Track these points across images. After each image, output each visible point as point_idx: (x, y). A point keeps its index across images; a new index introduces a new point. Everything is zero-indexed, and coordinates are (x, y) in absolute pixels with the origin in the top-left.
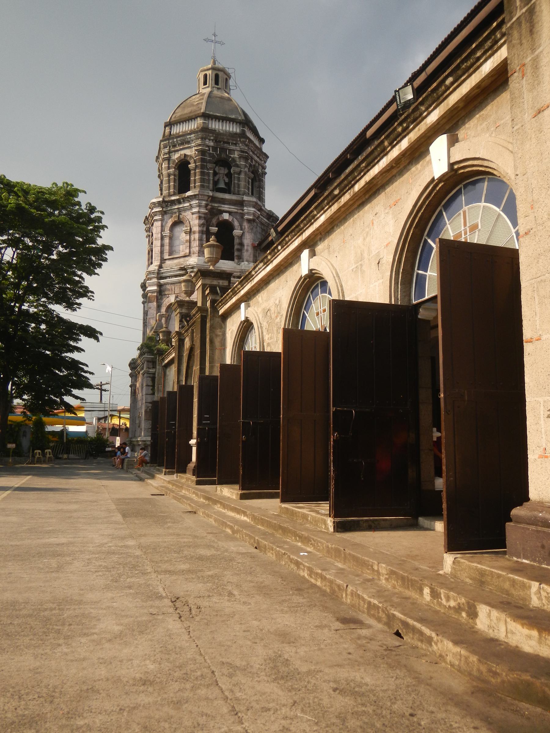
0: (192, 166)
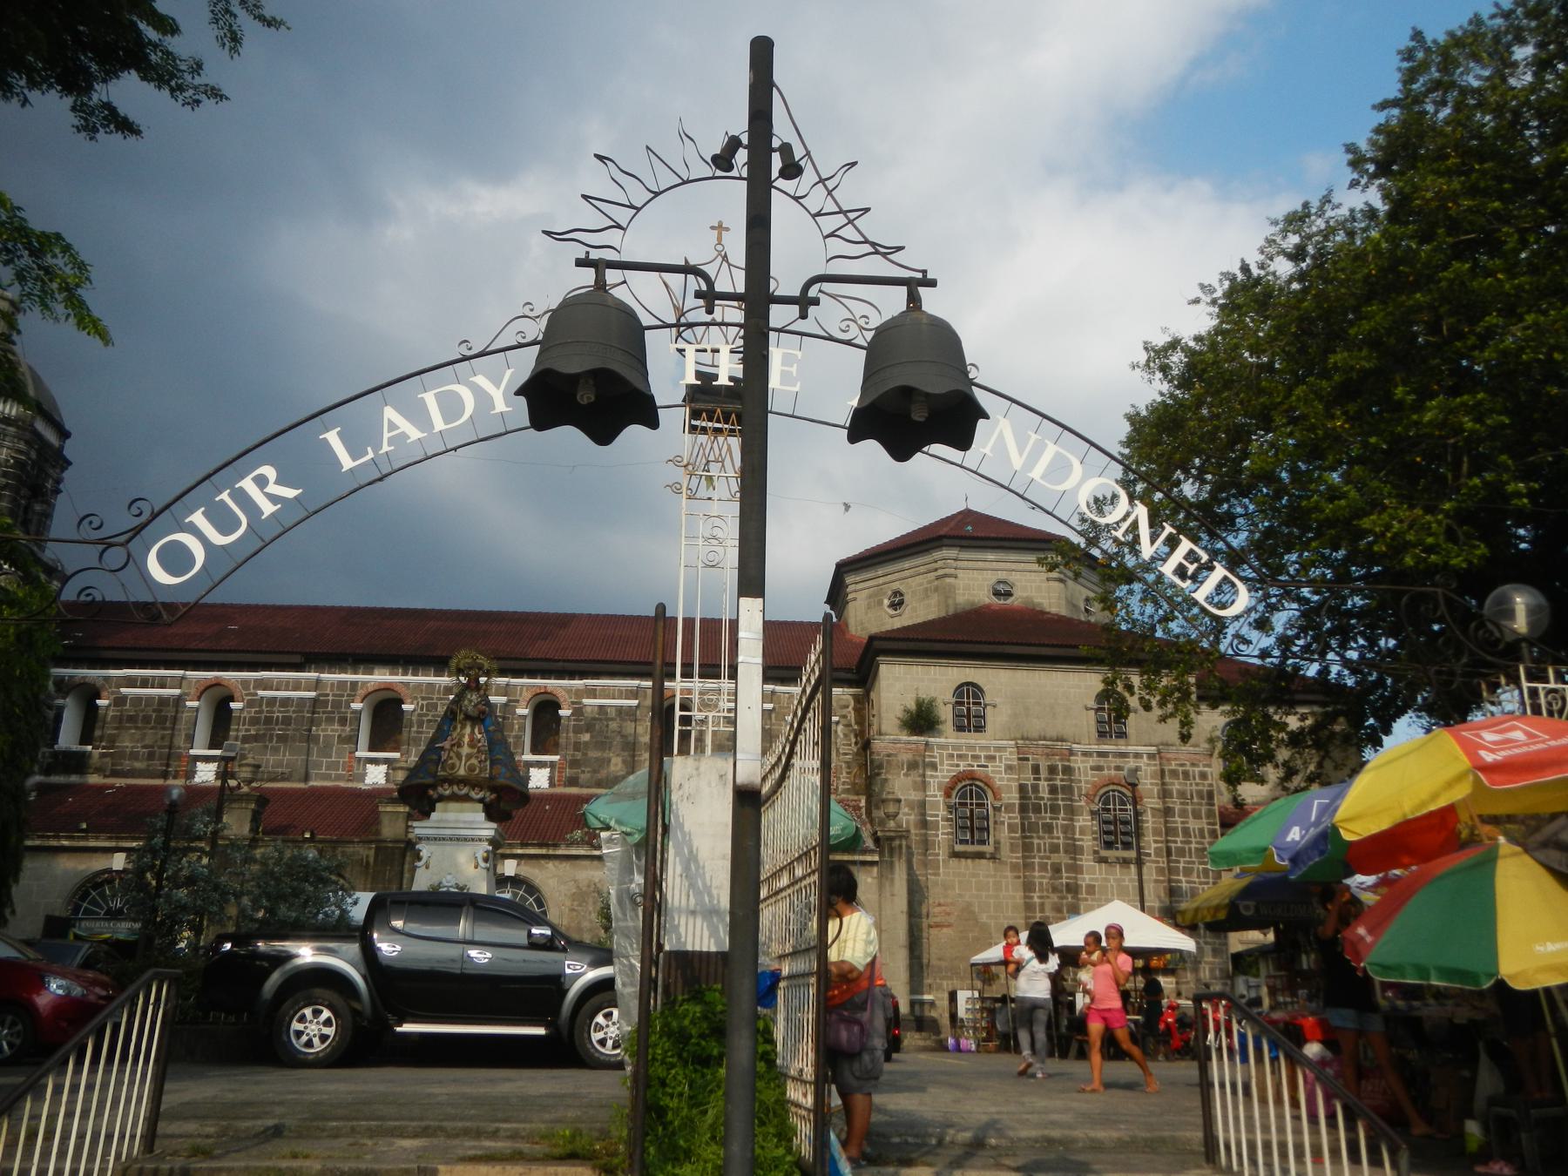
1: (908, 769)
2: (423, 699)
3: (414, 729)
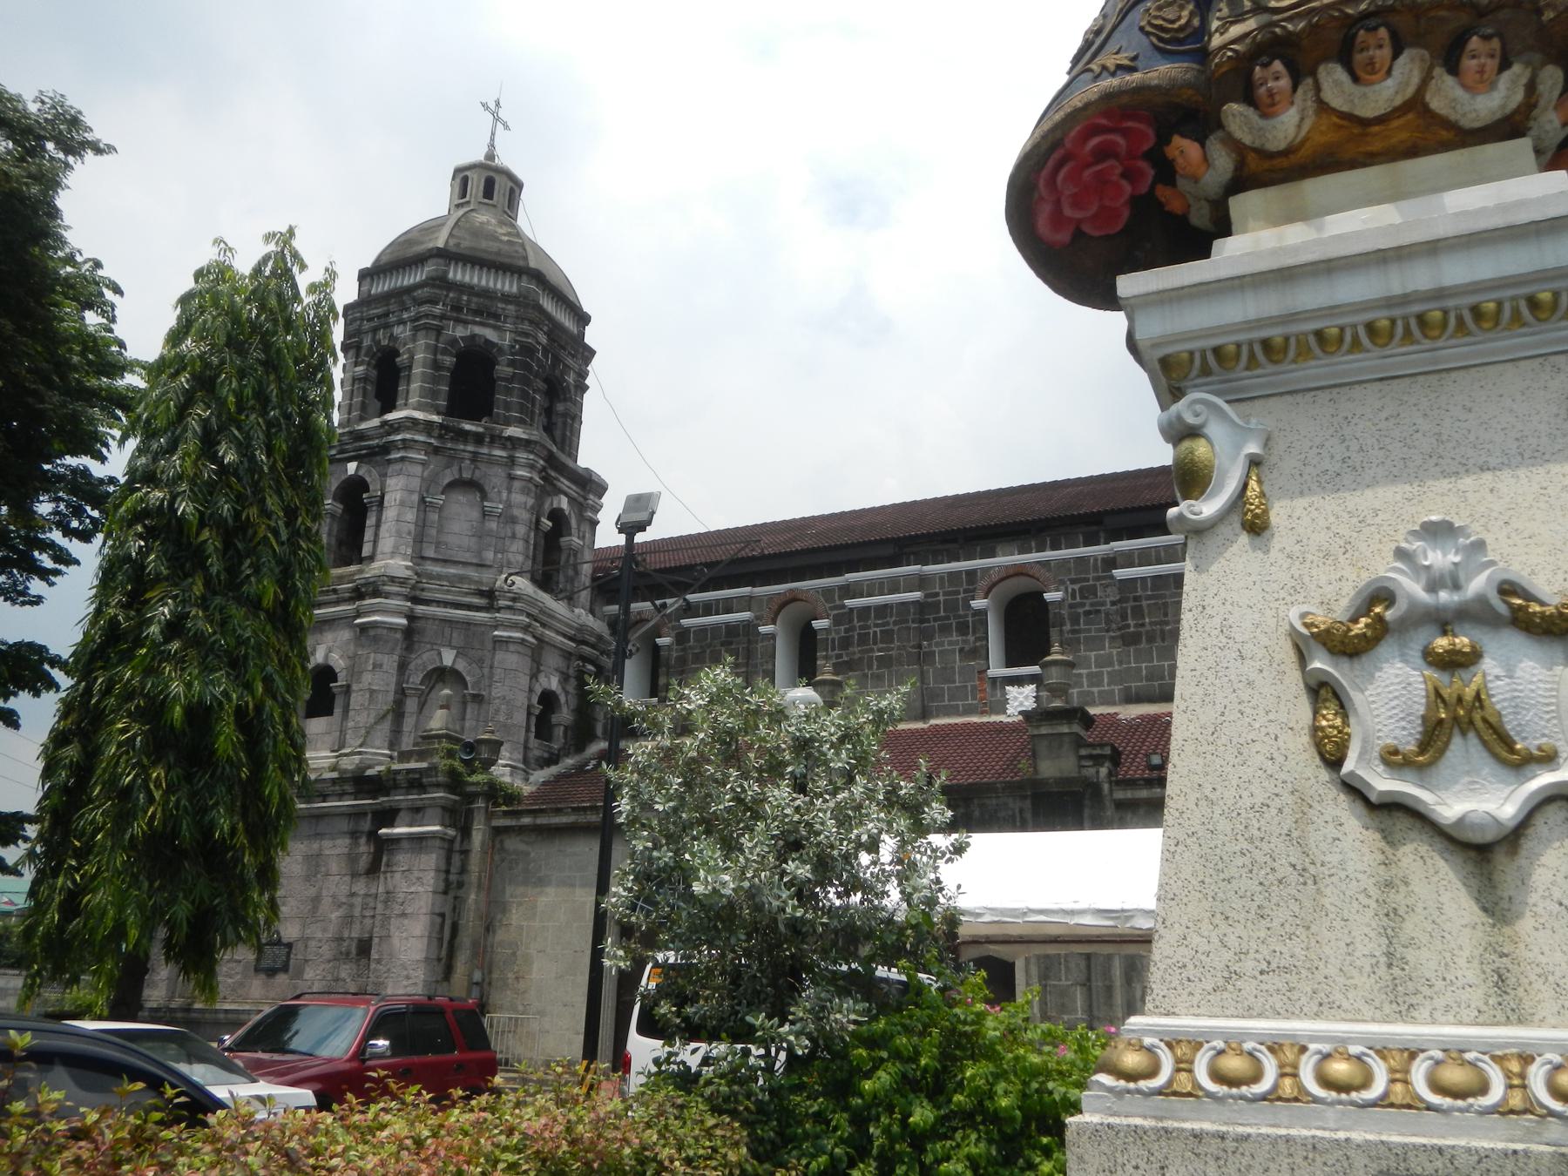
0: (503, 370)
2: (1073, 581)
3: (1068, 627)
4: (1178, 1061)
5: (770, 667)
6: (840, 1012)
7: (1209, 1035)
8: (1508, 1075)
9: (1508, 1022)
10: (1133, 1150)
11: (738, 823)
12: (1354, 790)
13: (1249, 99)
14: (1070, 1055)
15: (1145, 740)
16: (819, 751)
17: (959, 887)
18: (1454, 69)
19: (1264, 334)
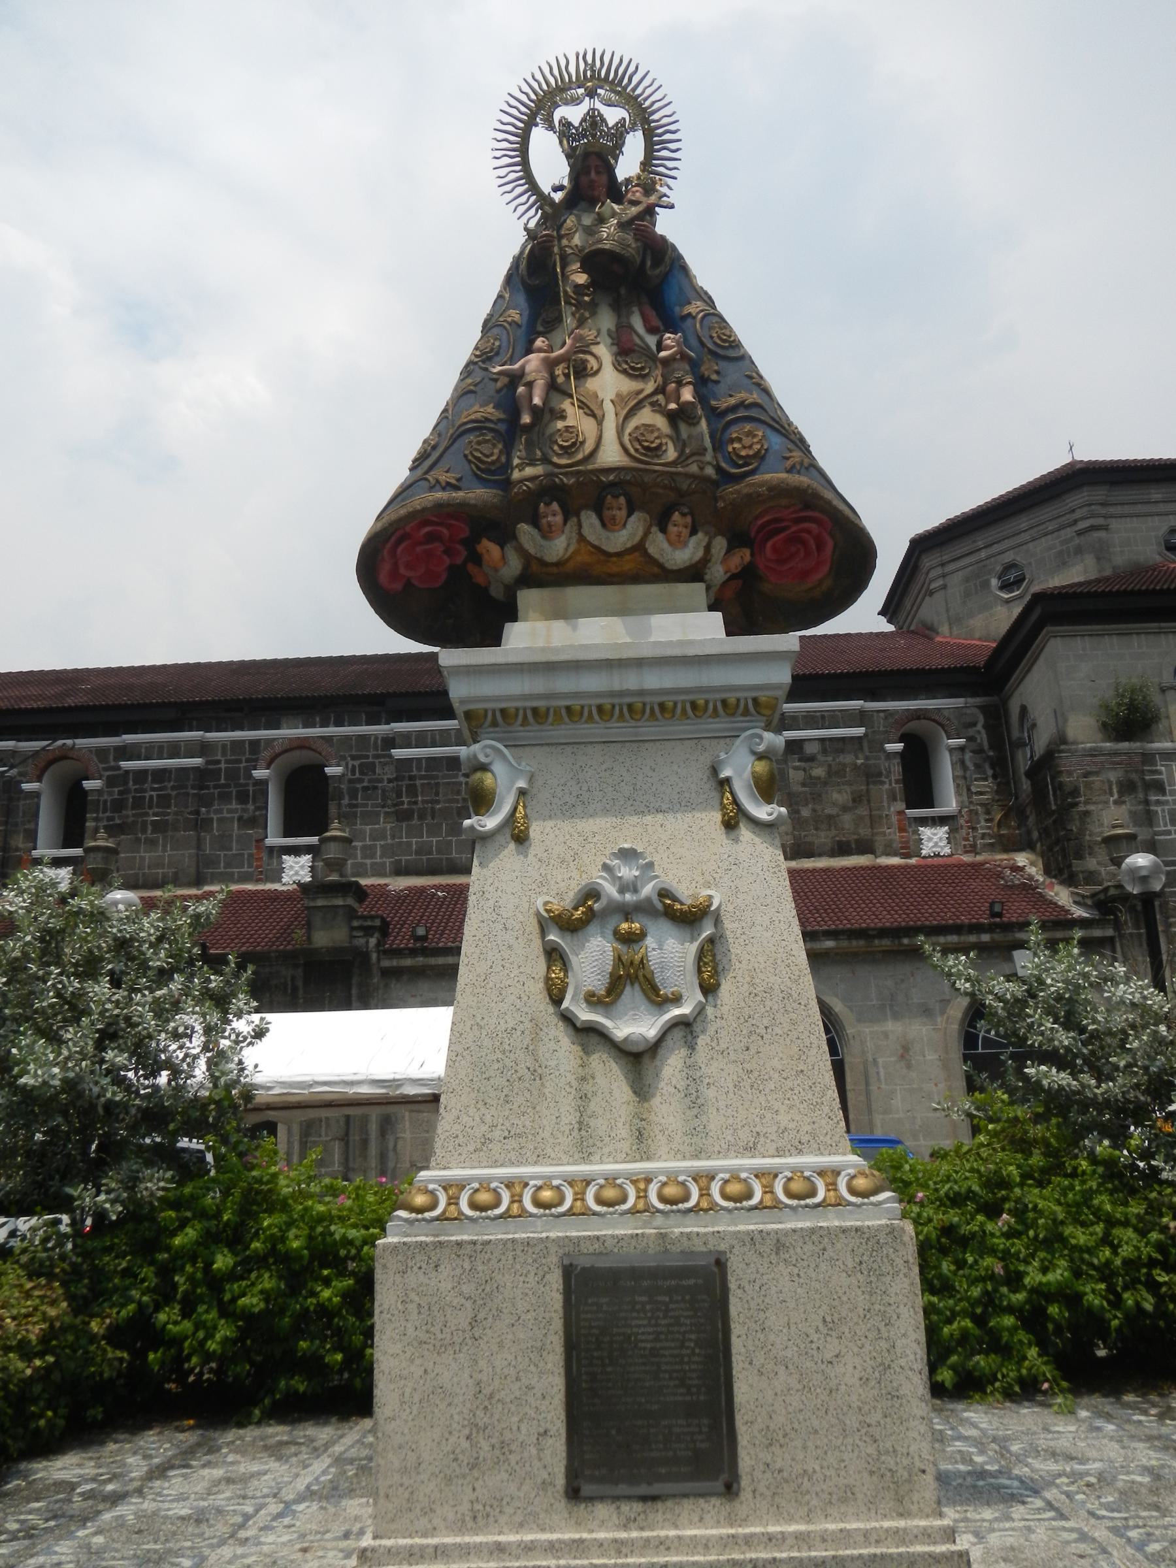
1: (1121, 793)
2: (353, 758)
3: (346, 801)
4: (450, 1198)
5: (31, 826)
6: (150, 1181)
7: (470, 1180)
8: (638, 1190)
9: (642, 1160)
10: (418, 1257)
11: (56, 1015)
12: (568, 1019)
13: (535, 521)
14: (349, 1203)
15: (411, 911)
16: (139, 951)
17: (256, 1066)
18: (663, 530)
19: (535, 704)
